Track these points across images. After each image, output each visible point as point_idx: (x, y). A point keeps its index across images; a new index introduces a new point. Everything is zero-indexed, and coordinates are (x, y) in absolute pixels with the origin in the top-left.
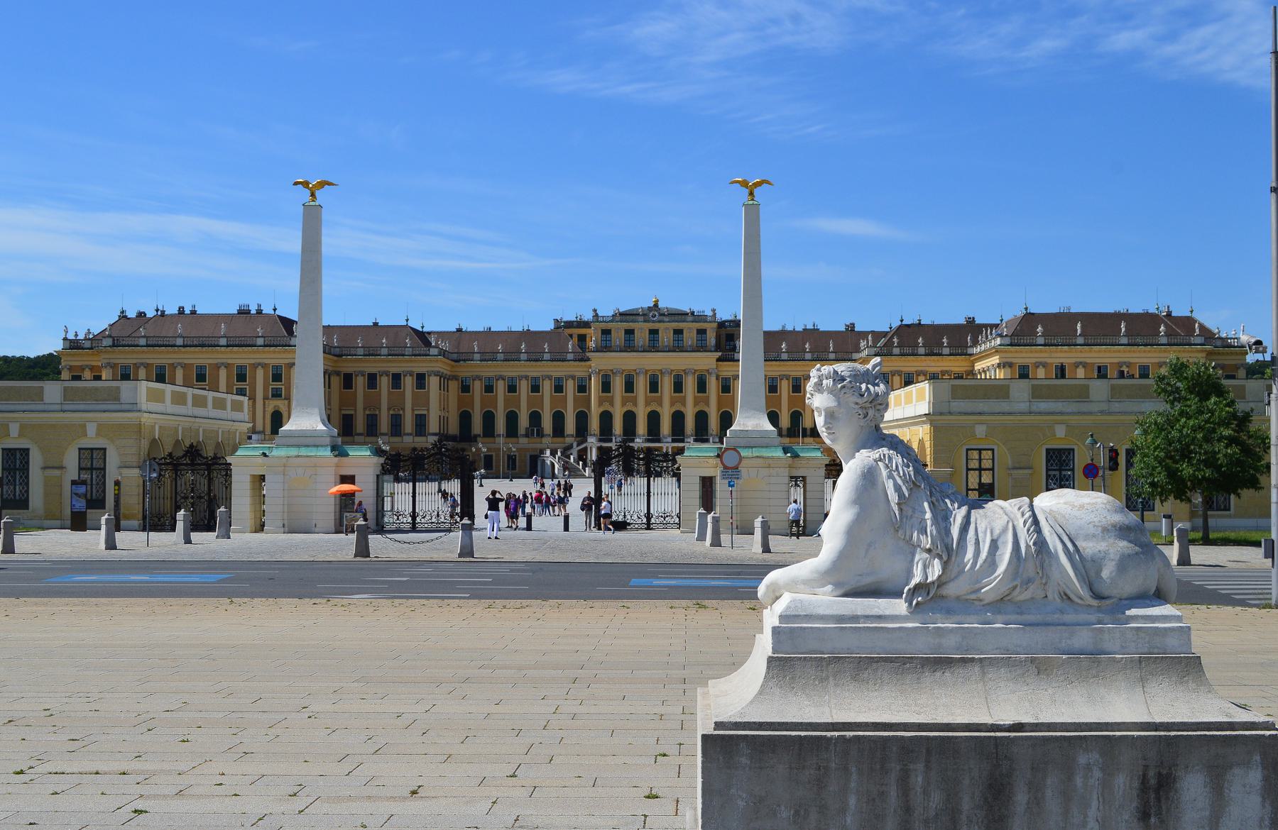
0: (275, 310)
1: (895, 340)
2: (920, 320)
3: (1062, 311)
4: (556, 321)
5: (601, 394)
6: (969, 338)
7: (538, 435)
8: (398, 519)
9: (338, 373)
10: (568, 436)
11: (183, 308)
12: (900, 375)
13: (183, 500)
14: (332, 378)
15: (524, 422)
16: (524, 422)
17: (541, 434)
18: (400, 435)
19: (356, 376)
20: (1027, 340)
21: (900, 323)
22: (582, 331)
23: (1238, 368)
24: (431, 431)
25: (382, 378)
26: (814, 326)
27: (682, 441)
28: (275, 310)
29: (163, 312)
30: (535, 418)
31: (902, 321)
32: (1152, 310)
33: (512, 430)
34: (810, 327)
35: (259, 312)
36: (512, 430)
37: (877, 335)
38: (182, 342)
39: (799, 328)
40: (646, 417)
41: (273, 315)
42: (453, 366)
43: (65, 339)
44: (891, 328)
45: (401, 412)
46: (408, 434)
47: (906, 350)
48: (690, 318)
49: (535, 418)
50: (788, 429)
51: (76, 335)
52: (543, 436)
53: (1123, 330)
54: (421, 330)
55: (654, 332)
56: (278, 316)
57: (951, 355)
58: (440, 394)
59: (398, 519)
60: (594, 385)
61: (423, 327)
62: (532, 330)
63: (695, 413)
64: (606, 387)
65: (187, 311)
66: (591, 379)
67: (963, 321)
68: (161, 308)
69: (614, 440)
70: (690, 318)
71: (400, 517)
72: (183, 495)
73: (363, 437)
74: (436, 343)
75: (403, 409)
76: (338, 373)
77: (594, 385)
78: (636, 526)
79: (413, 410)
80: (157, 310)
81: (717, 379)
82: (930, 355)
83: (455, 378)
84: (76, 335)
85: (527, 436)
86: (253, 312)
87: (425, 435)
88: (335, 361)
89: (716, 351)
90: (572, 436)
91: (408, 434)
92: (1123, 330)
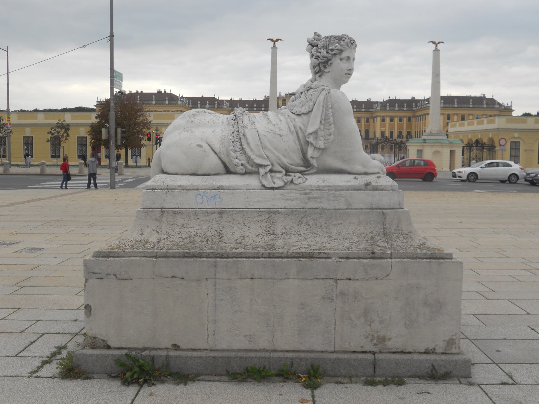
0: (171, 91)
2: (396, 98)
4: (265, 96)
12: (389, 117)
28: (171, 91)
29: (131, 92)
34: (354, 100)
35: (165, 92)
43: (97, 101)
47: (391, 108)
51: (100, 100)
65: (140, 92)
67: (410, 98)
68: (130, 91)
80: (129, 91)
84: (100, 100)
86: (163, 92)
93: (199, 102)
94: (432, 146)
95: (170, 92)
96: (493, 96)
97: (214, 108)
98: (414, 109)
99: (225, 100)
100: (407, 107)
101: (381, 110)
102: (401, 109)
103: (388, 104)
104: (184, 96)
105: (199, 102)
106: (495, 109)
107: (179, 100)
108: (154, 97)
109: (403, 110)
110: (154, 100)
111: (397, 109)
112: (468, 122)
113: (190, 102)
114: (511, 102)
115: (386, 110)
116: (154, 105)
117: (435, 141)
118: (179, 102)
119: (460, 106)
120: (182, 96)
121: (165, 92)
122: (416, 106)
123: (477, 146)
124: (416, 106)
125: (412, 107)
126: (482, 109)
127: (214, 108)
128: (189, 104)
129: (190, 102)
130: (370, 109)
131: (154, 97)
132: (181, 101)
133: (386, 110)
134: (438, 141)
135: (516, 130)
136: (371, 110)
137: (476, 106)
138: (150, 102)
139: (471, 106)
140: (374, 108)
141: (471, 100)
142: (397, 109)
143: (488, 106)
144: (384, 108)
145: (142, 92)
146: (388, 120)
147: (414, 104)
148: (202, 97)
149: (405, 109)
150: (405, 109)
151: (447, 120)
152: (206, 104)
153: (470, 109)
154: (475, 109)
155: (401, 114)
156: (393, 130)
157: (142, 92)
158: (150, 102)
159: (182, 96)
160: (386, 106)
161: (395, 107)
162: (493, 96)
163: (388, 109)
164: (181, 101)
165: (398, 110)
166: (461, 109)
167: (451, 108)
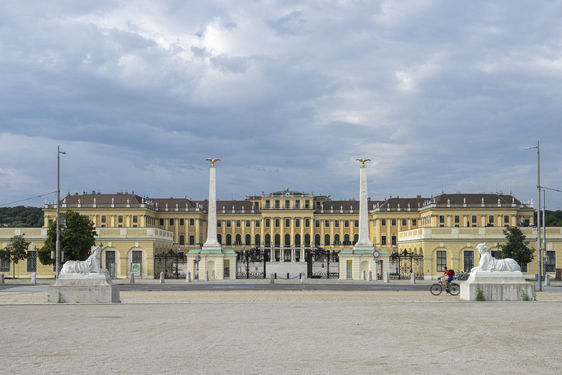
0: (133, 193)
1: (388, 205)
3: (457, 193)
5: (266, 227)
6: (419, 204)
7: (239, 244)
8: (242, 275)
9: (158, 219)
10: (252, 244)
11: (95, 191)
13: (168, 269)
14: (155, 221)
15: (233, 239)
16: (233, 239)
17: (240, 244)
18: (250, 245)
19: (165, 220)
20: (443, 205)
21: (390, 198)
22: (257, 201)
23: (530, 217)
24: (196, 243)
25: (166, 221)
26: (353, 198)
27: (300, 246)
28: (133, 193)
30: (238, 237)
31: (391, 197)
32: (495, 193)
33: (248, 242)
34: (352, 199)
36: (248, 242)
37: (381, 203)
38: (112, 206)
39: (347, 200)
40: (284, 237)
41: (133, 195)
42: (204, 216)
44: (385, 200)
46: (187, 244)
47: (393, 209)
48: (302, 196)
49: (238, 237)
50: (353, 242)
52: (242, 245)
53: (483, 201)
54: (190, 200)
55: (288, 202)
56: (135, 195)
57: (411, 211)
58: (200, 227)
59: (242, 275)
60: (262, 224)
61: (191, 199)
62: (236, 200)
63: (295, 235)
64: (268, 224)
65: (96, 193)
66: (261, 221)
67: (416, 197)
69: (271, 246)
70: (302, 196)
71: (243, 274)
72: (168, 267)
73: (188, 245)
74: (198, 206)
75: (185, 234)
76: (158, 219)
77: (262, 224)
78: (324, 277)
79: (189, 234)
80: (84, 193)
81: (314, 221)
82: (403, 211)
85: (235, 244)
87: (194, 244)
88: (157, 214)
89: (313, 209)
90: (254, 244)
91: (187, 244)
92: (483, 201)
94: (360, 256)
99: (198, 202)
101: (380, 211)
102: (405, 209)
106: (512, 209)
109: (407, 211)
112: (409, 232)
115: (386, 211)
117: (363, 252)
119: (469, 206)
123: (405, 256)
126: (496, 209)
133: (386, 211)
134: (366, 252)
135: (442, 240)
137: (489, 205)
140: (374, 208)
143: (504, 206)
146: (389, 223)
151: (440, 222)
153: (482, 209)
154: (488, 209)
155: (404, 216)
156: (396, 235)
164: (144, 203)
165: (401, 211)
166: (471, 209)
167: (459, 209)
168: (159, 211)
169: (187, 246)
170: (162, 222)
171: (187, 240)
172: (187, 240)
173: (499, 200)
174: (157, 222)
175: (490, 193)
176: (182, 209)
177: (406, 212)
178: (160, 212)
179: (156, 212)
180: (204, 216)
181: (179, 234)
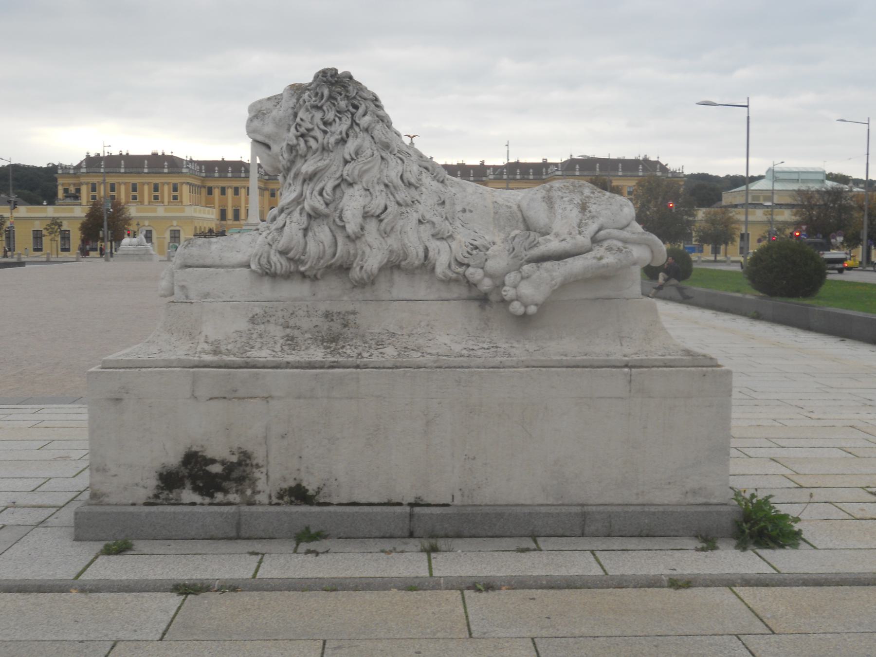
19: (215, 188)
45: (239, 208)
47: (511, 177)
65: (124, 153)
75: (240, 207)
76: (205, 187)
83: (267, 189)
91: (243, 220)
93: (217, 169)
95: (170, 154)
96: (658, 158)
97: (240, 177)
98: (544, 177)
100: (534, 174)
102: (526, 177)
103: (505, 170)
104: (195, 159)
105: (217, 169)
107: (185, 167)
108: (146, 162)
110: (146, 167)
111: (518, 177)
113: (203, 167)
114: (683, 166)
116: (146, 175)
118: (184, 170)
120: (191, 159)
121: (163, 154)
122: (547, 174)
124: (547, 174)
125: (542, 174)
127: (240, 177)
128: (201, 171)
129: (203, 167)
130: (482, 177)
131: (146, 162)
132: (187, 168)
133: (502, 179)
136: (484, 179)
137: (629, 174)
138: (140, 170)
139: (620, 174)
141: (620, 165)
142: (518, 177)
144: (498, 176)
145: (127, 154)
147: (544, 170)
148: (223, 159)
149: (531, 177)
150: (531, 177)
152: (227, 172)
157: (127, 154)
158: (140, 170)
159: (191, 159)
160: (502, 173)
161: (516, 174)
162: (658, 158)
163: (505, 177)
164: (187, 168)
165: (521, 179)
168: (206, 177)
169: (230, 222)
170: (210, 191)
171: (230, 214)
172: (230, 214)
173: (641, 167)
174: (204, 191)
175: (634, 158)
176: (237, 175)
177: (526, 181)
178: (207, 179)
179: (202, 178)
180: (265, 183)
181: (232, 207)
